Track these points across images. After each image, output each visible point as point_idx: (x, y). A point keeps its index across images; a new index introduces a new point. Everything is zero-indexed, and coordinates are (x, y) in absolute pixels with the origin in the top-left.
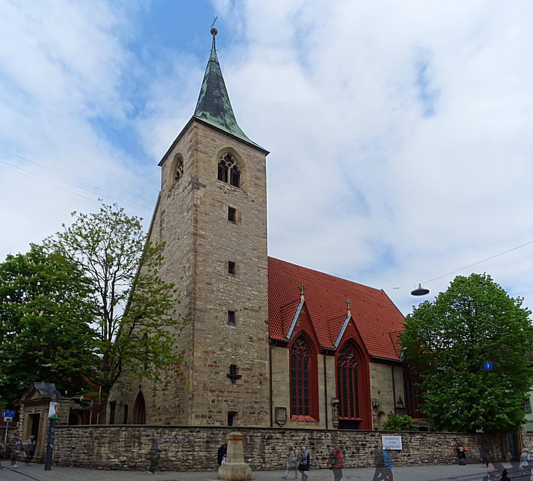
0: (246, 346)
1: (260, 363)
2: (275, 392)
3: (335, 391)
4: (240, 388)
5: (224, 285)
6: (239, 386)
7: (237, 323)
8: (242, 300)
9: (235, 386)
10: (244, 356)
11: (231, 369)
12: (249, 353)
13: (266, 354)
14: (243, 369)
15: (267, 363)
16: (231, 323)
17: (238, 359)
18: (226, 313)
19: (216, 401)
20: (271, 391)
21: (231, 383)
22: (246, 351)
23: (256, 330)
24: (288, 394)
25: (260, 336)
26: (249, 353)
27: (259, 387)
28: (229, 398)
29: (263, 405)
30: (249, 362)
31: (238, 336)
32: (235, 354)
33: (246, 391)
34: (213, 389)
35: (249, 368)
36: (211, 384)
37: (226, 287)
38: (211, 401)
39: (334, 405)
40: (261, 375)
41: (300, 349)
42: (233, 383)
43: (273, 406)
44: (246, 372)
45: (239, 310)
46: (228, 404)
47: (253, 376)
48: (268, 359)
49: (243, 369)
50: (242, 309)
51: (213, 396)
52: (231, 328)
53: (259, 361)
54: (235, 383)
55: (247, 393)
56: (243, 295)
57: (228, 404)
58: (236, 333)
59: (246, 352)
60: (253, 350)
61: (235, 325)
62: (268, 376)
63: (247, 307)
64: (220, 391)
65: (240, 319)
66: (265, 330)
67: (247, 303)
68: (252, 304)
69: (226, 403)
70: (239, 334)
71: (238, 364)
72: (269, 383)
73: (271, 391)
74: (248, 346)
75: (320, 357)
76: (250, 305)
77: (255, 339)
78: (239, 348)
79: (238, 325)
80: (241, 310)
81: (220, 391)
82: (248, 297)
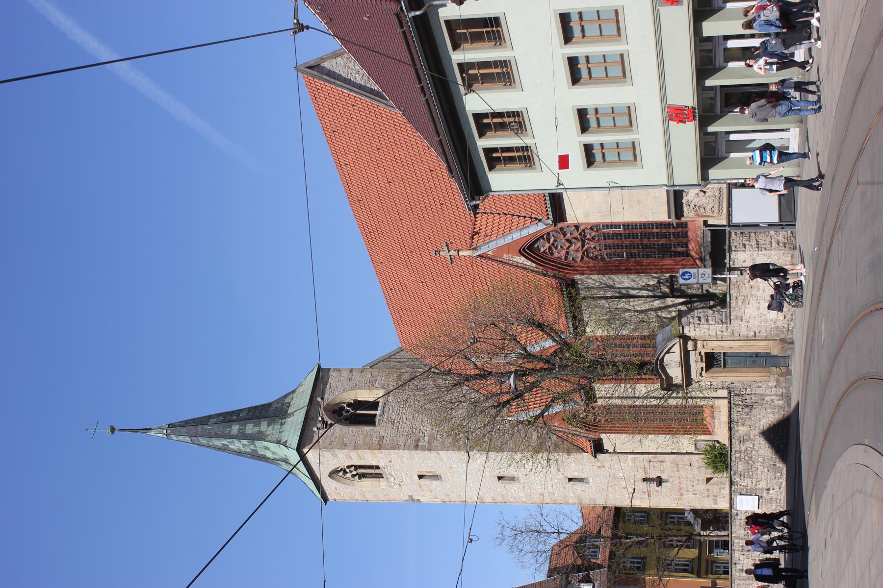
64: (681, 489)
69: (695, 486)
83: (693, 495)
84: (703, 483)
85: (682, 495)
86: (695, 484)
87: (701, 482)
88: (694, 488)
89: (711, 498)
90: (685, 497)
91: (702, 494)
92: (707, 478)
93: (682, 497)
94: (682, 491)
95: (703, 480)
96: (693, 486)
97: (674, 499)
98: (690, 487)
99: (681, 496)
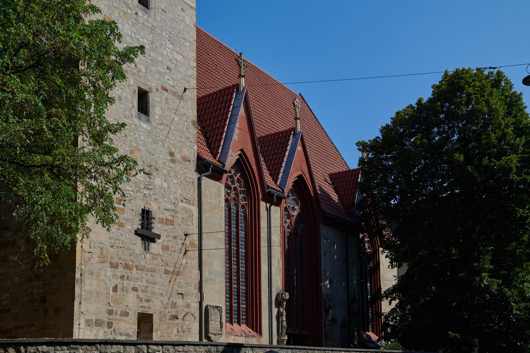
1: (184, 209)
2: (205, 274)
3: (281, 276)
4: (157, 262)
5: (133, 28)
6: (155, 256)
7: (151, 118)
8: (159, 68)
9: (148, 255)
11: (143, 217)
12: (169, 187)
13: (194, 192)
14: (161, 221)
15: (195, 210)
16: (143, 116)
18: (135, 91)
19: (119, 288)
21: (142, 250)
22: (165, 181)
23: (180, 139)
27: (184, 262)
28: (139, 283)
29: (190, 301)
30: (169, 206)
31: (153, 146)
32: (149, 187)
33: (165, 270)
34: (115, 261)
35: (170, 218)
36: (112, 250)
37: (135, 34)
38: (111, 289)
39: (279, 304)
41: (235, 189)
42: (146, 249)
43: (203, 303)
44: (165, 226)
45: (154, 89)
46: (138, 297)
48: (196, 202)
49: (161, 221)
50: (160, 88)
51: (115, 276)
52: (143, 128)
54: (148, 250)
55: (167, 272)
56: (160, 59)
57: (138, 297)
58: (150, 141)
59: (165, 185)
60: (175, 181)
61: (148, 121)
62: (196, 237)
63: (167, 86)
64: (127, 267)
65: (156, 111)
66: (193, 141)
67: (166, 77)
68: (173, 80)
69: (135, 293)
70: (155, 142)
71: (154, 207)
72: (197, 253)
75: (263, 204)
76: (171, 83)
77: (178, 156)
79: (154, 124)
80: (157, 90)
81: (127, 267)
82: (168, 63)
83: (113, 285)
84: (142, 307)
85: (114, 266)
86: (140, 293)
87: (144, 304)
88: (130, 291)
89: (105, 317)
90: (109, 270)
91: (116, 302)
92: (152, 315)
93: (108, 265)
94: (120, 269)
96: (135, 289)
97: (102, 249)
98: (132, 284)
99: (111, 263)
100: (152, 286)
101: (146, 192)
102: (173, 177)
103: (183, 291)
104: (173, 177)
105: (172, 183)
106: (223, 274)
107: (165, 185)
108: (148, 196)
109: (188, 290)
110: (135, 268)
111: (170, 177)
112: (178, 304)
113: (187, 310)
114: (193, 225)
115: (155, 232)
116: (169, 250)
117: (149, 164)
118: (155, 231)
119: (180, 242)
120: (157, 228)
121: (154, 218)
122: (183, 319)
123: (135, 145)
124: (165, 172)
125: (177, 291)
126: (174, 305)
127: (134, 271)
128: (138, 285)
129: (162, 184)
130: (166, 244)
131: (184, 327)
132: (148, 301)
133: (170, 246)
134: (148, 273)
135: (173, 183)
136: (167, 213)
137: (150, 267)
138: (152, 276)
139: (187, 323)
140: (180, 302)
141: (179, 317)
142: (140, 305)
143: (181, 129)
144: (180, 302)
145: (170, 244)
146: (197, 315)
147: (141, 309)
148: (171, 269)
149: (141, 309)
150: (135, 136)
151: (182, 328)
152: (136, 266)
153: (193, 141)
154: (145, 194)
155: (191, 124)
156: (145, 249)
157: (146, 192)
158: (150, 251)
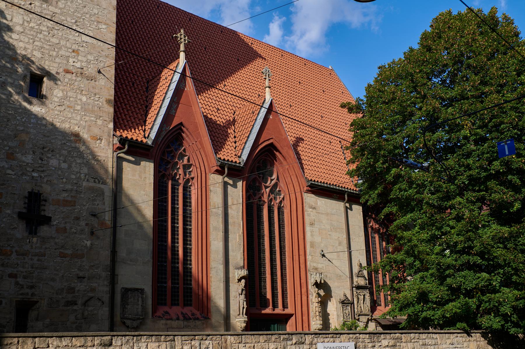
0: (65, 152)
2: (122, 253)
9: (35, 240)
10: (60, 172)
12: (70, 167)
17: (45, 180)
20: (114, 252)
22: (64, 162)
24: (148, 257)
25: (96, 131)
26: (70, 167)
27: (89, 243)
30: (69, 187)
32: (40, 169)
35: (69, 199)
40: (94, 215)
46: (17, 283)
47: (77, 219)
53: (91, 184)
54: (36, 234)
55: (63, 256)
57: (17, 283)
59: (64, 166)
62: (108, 217)
71: (46, 189)
73: (114, 252)
74: (69, 152)
78: (49, 155)
84: (22, 294)
95: (33, 294)
96: (11, 276)
100: (38, 271)
101: (35, 174)
102: (76, 157)
103: (87, 275)
104: (76, 157)
105: (74, 164)
106: (150, 253)
107: (64, 166)
108: (39, 179)
109: (94, 273)
110: (14, 254)
111: (72, 157)
112: (77, 289)
113: (91, 294)
114: (104, 204)
115: (47, 215)
116: (66, 232)
117: (42, 146)
118: (48, 214)
119: (83, 223)
120: (49, 210)
121: (46, 201)
122: (85, 304)
123: (22, 128)
124: (65, 152)
125: (77, 274)
126: (71, 290)
127: (14, 256)
128: (17, 271)
129: (59, 165)
130: (62, 226)
131: (86, 313)
132: (32, 287)
133: (68, 228)
134: (33, 258)
135: (77, 163)
136: (65, 195)
137: (37, 251)
138: (38, 260)
139: (90, 309)
140: (81, 286)
141: (80, 302)
142: (21, 292)
143: (91, 109)
144: (81, 286)
145: (68, 226)
146: (106, 298)
147: (21, 297)
148: (69, 252)
149: (21, 297)
150: (23, 120)
151: (83, 314)
152: (16, 251)
153: (107, 119)
154: (33, 177)
155: (105, 103)
156: (30, 233)
157: (35, 174)
158: (38, 234)
